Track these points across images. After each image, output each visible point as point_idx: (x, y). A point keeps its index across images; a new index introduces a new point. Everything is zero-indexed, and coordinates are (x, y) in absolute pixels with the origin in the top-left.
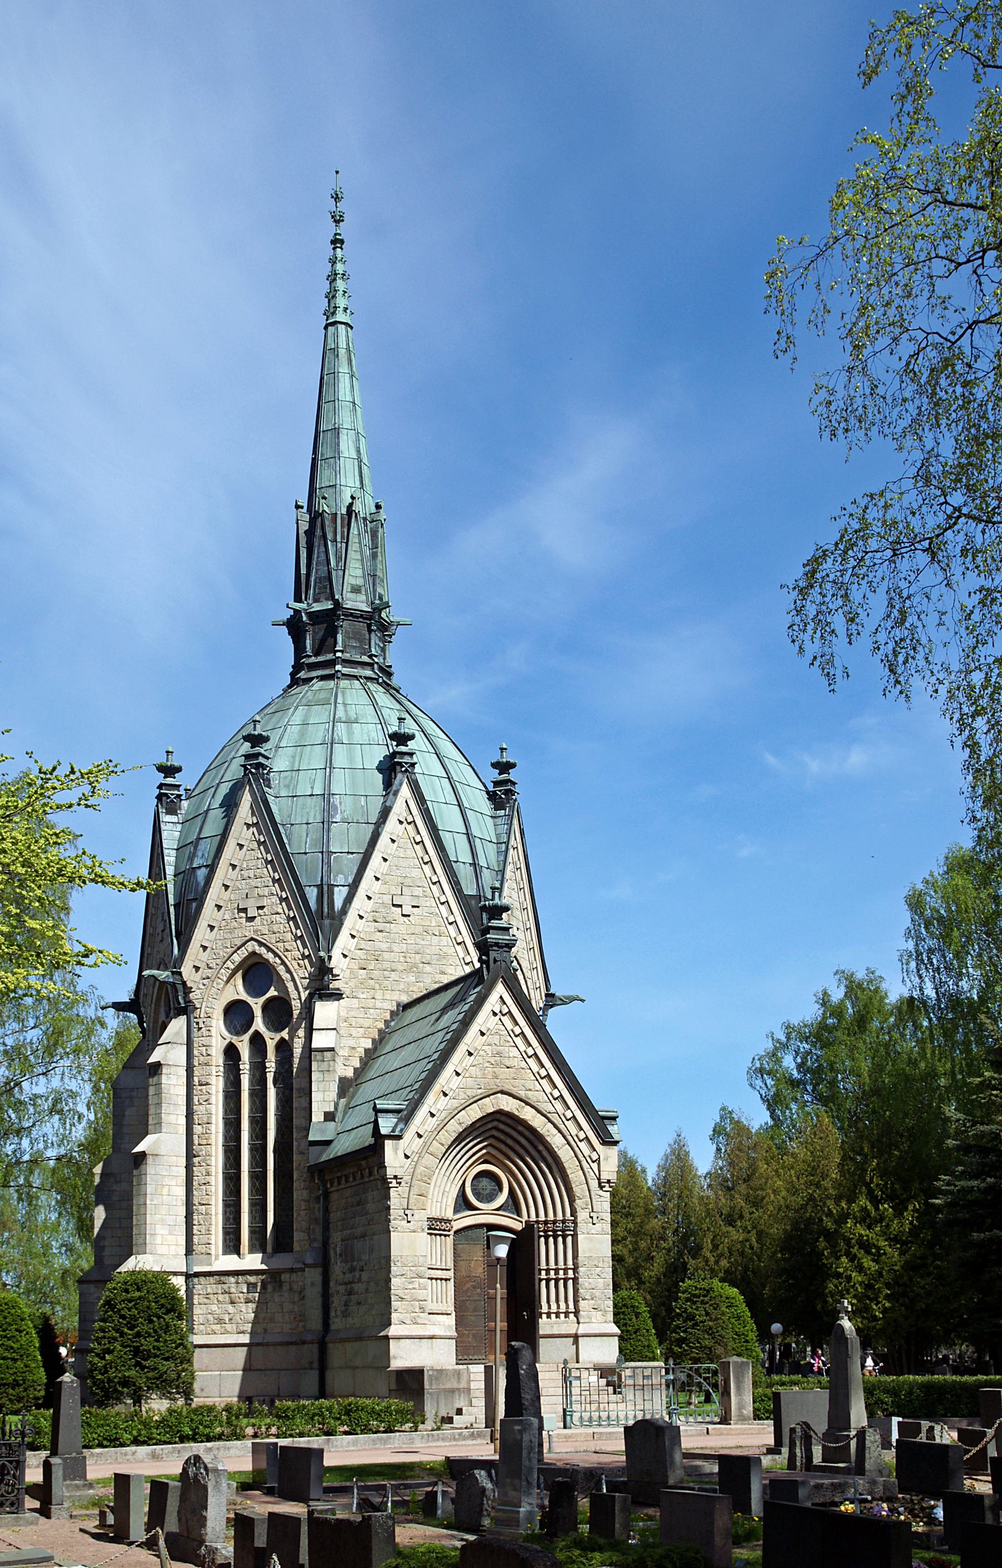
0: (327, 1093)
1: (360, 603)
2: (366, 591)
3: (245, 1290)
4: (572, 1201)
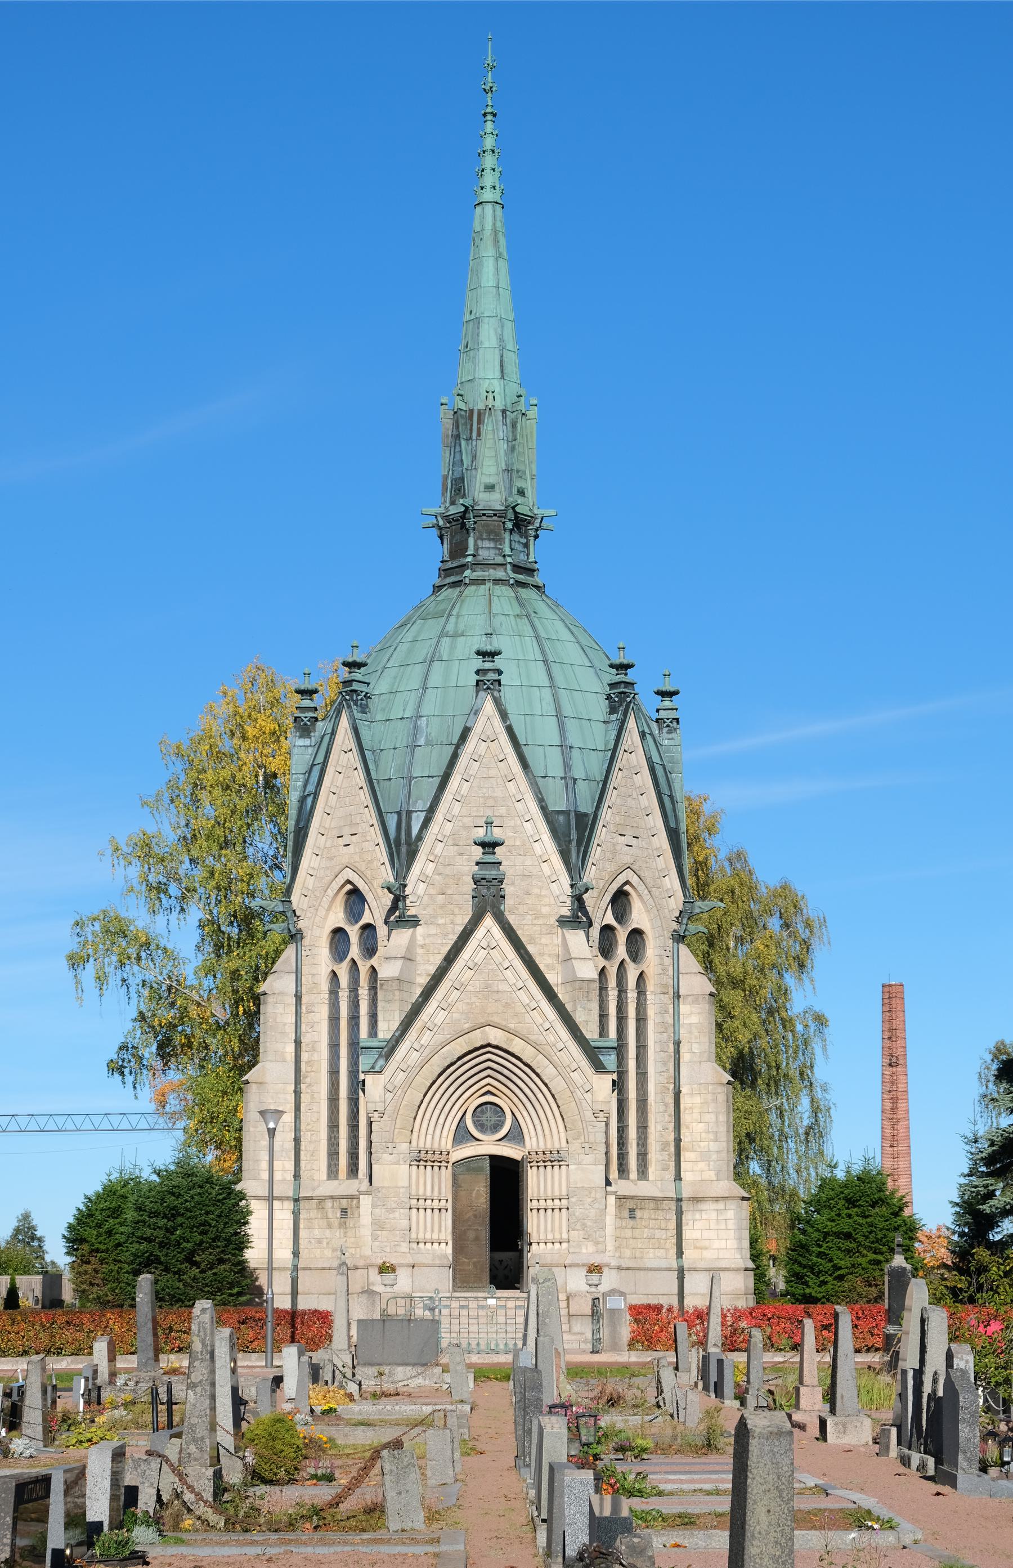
0: (391, 1023)
1: (495, 501)
2: (500, 488)
3: (339, 1216)
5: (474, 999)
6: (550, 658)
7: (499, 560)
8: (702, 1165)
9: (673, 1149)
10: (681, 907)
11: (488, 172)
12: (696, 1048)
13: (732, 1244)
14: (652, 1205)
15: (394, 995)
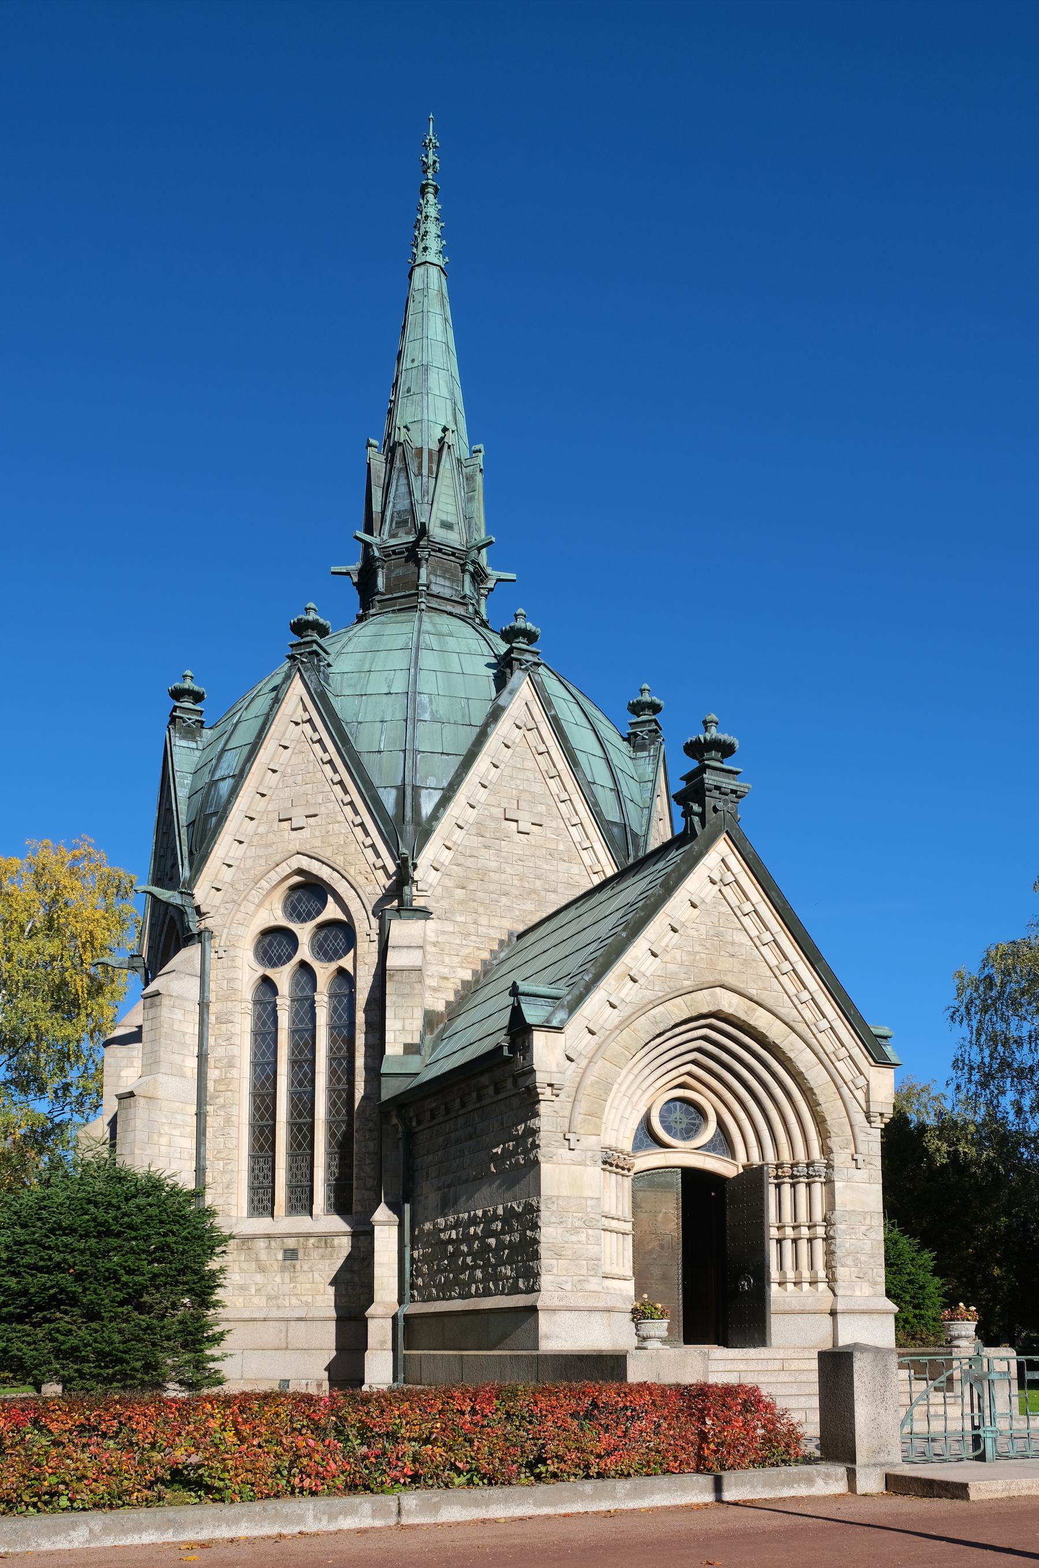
4: (824, 1134)
5: (698, 948)
15: (413, 988)
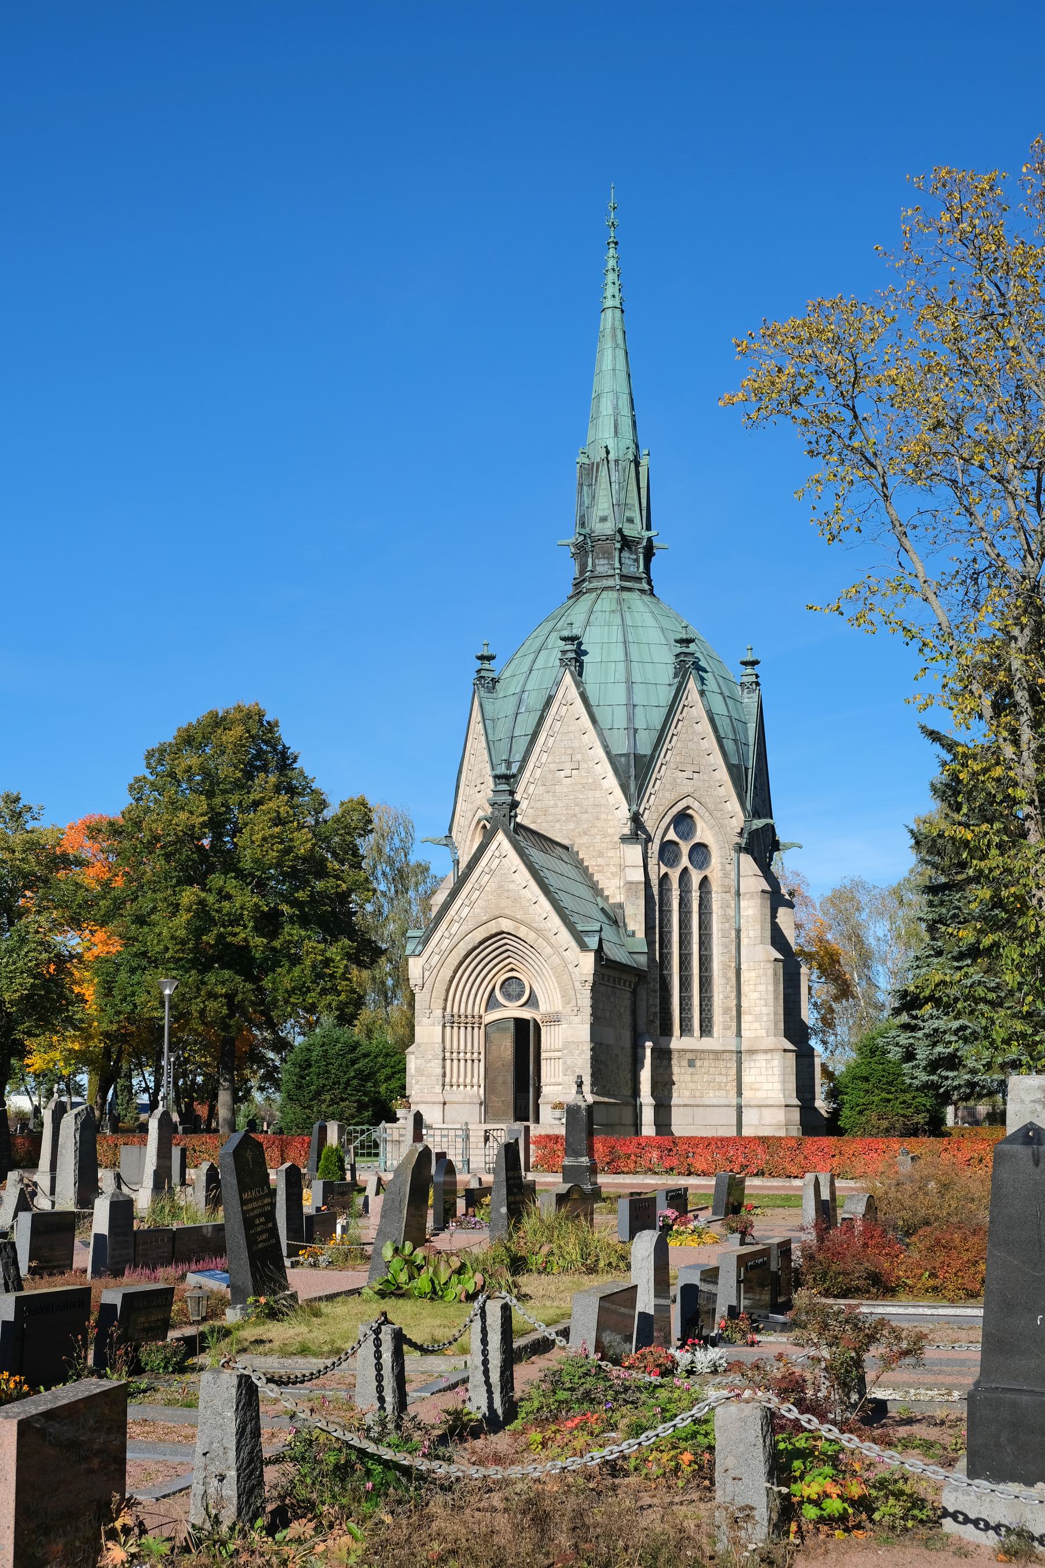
6: (630, 640)
7: (611, 572)
8: (756, 1025)
9: (734, 1013)
10: (742, 825)
11: (610, 285)
12: (752, 934)
13: (778, 1086)
14: (711, 1056)
